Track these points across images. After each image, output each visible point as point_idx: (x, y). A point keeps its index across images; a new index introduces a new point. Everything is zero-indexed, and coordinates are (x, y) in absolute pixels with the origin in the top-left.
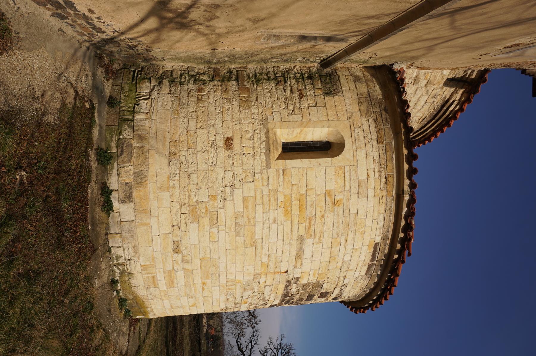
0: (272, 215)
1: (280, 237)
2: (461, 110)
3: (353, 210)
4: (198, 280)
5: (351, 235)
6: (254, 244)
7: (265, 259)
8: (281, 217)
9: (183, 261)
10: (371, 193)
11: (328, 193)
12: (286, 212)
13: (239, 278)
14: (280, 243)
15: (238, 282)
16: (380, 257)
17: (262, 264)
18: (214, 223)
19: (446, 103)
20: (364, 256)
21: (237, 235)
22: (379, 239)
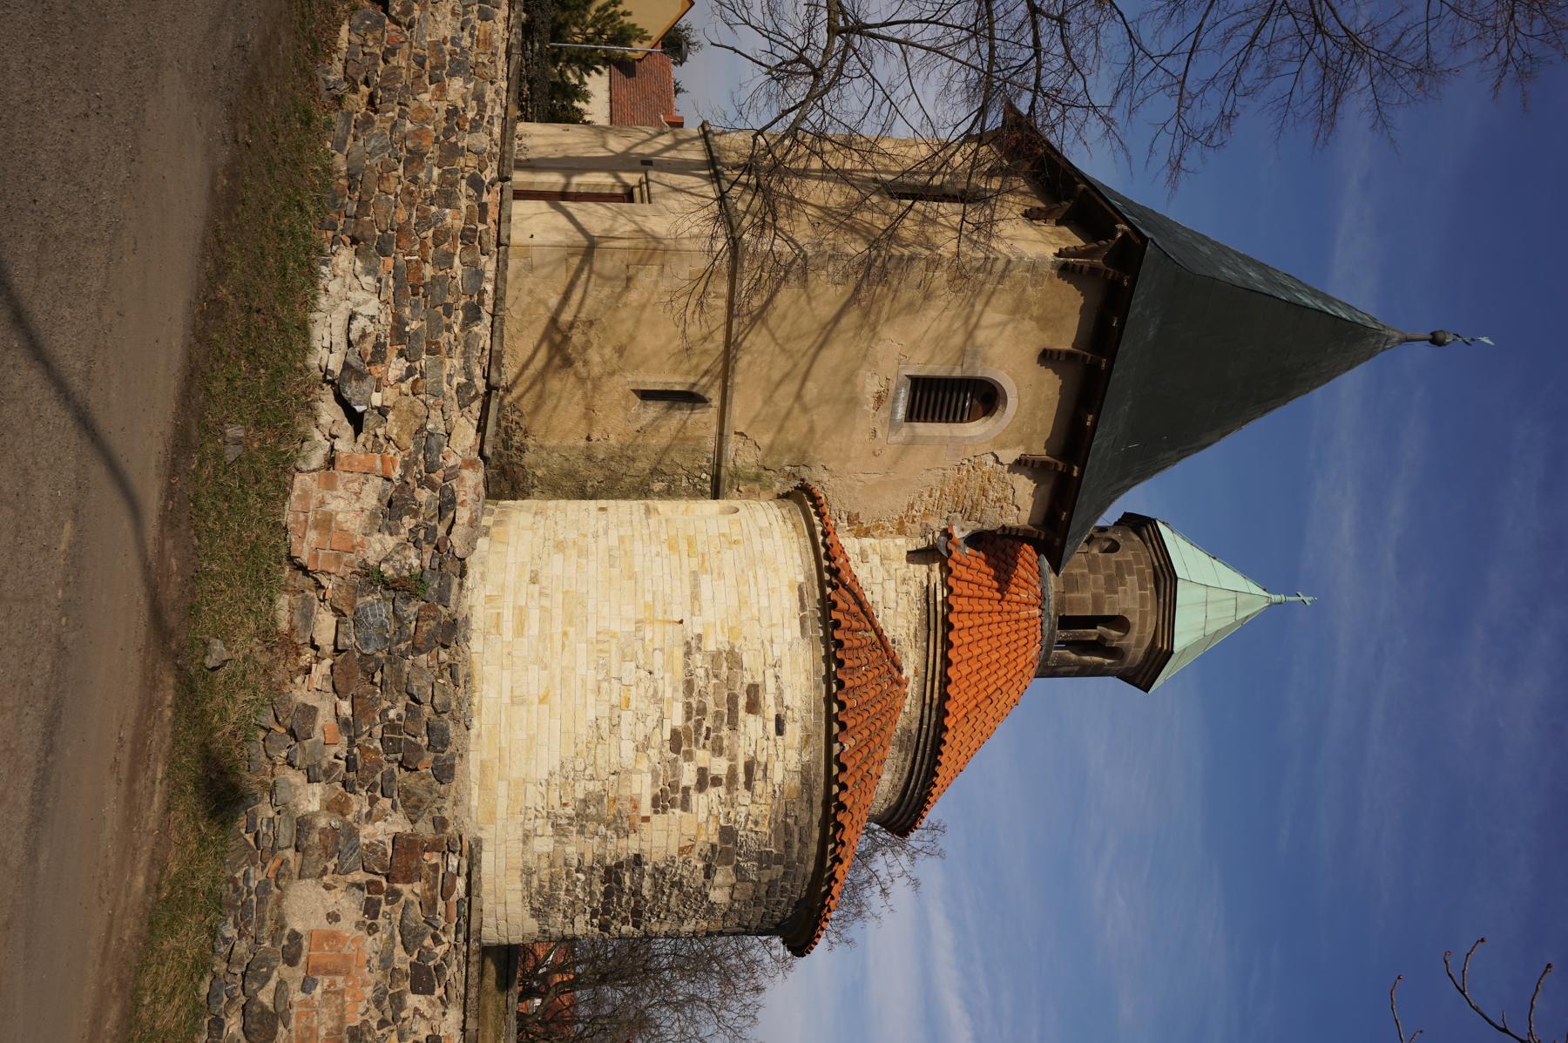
0: (654, 549)
1: (666, 570)
2: (950, 590)
3: (758, 548)
4: (558, 628)
5: (760, 572)
6: (632, 576)
7: (649, 598)
8: (666, 551)
9: (541, 594)
10: (777, 535)
12: (671, 547)
14: (667, 577)
15: (614, 636)
16: (812, 604)
17: (646, 606)
18: (583, 553)
19: (928, 593)
20: (790, 601)
21: (611, 566)
22: (801, 579)
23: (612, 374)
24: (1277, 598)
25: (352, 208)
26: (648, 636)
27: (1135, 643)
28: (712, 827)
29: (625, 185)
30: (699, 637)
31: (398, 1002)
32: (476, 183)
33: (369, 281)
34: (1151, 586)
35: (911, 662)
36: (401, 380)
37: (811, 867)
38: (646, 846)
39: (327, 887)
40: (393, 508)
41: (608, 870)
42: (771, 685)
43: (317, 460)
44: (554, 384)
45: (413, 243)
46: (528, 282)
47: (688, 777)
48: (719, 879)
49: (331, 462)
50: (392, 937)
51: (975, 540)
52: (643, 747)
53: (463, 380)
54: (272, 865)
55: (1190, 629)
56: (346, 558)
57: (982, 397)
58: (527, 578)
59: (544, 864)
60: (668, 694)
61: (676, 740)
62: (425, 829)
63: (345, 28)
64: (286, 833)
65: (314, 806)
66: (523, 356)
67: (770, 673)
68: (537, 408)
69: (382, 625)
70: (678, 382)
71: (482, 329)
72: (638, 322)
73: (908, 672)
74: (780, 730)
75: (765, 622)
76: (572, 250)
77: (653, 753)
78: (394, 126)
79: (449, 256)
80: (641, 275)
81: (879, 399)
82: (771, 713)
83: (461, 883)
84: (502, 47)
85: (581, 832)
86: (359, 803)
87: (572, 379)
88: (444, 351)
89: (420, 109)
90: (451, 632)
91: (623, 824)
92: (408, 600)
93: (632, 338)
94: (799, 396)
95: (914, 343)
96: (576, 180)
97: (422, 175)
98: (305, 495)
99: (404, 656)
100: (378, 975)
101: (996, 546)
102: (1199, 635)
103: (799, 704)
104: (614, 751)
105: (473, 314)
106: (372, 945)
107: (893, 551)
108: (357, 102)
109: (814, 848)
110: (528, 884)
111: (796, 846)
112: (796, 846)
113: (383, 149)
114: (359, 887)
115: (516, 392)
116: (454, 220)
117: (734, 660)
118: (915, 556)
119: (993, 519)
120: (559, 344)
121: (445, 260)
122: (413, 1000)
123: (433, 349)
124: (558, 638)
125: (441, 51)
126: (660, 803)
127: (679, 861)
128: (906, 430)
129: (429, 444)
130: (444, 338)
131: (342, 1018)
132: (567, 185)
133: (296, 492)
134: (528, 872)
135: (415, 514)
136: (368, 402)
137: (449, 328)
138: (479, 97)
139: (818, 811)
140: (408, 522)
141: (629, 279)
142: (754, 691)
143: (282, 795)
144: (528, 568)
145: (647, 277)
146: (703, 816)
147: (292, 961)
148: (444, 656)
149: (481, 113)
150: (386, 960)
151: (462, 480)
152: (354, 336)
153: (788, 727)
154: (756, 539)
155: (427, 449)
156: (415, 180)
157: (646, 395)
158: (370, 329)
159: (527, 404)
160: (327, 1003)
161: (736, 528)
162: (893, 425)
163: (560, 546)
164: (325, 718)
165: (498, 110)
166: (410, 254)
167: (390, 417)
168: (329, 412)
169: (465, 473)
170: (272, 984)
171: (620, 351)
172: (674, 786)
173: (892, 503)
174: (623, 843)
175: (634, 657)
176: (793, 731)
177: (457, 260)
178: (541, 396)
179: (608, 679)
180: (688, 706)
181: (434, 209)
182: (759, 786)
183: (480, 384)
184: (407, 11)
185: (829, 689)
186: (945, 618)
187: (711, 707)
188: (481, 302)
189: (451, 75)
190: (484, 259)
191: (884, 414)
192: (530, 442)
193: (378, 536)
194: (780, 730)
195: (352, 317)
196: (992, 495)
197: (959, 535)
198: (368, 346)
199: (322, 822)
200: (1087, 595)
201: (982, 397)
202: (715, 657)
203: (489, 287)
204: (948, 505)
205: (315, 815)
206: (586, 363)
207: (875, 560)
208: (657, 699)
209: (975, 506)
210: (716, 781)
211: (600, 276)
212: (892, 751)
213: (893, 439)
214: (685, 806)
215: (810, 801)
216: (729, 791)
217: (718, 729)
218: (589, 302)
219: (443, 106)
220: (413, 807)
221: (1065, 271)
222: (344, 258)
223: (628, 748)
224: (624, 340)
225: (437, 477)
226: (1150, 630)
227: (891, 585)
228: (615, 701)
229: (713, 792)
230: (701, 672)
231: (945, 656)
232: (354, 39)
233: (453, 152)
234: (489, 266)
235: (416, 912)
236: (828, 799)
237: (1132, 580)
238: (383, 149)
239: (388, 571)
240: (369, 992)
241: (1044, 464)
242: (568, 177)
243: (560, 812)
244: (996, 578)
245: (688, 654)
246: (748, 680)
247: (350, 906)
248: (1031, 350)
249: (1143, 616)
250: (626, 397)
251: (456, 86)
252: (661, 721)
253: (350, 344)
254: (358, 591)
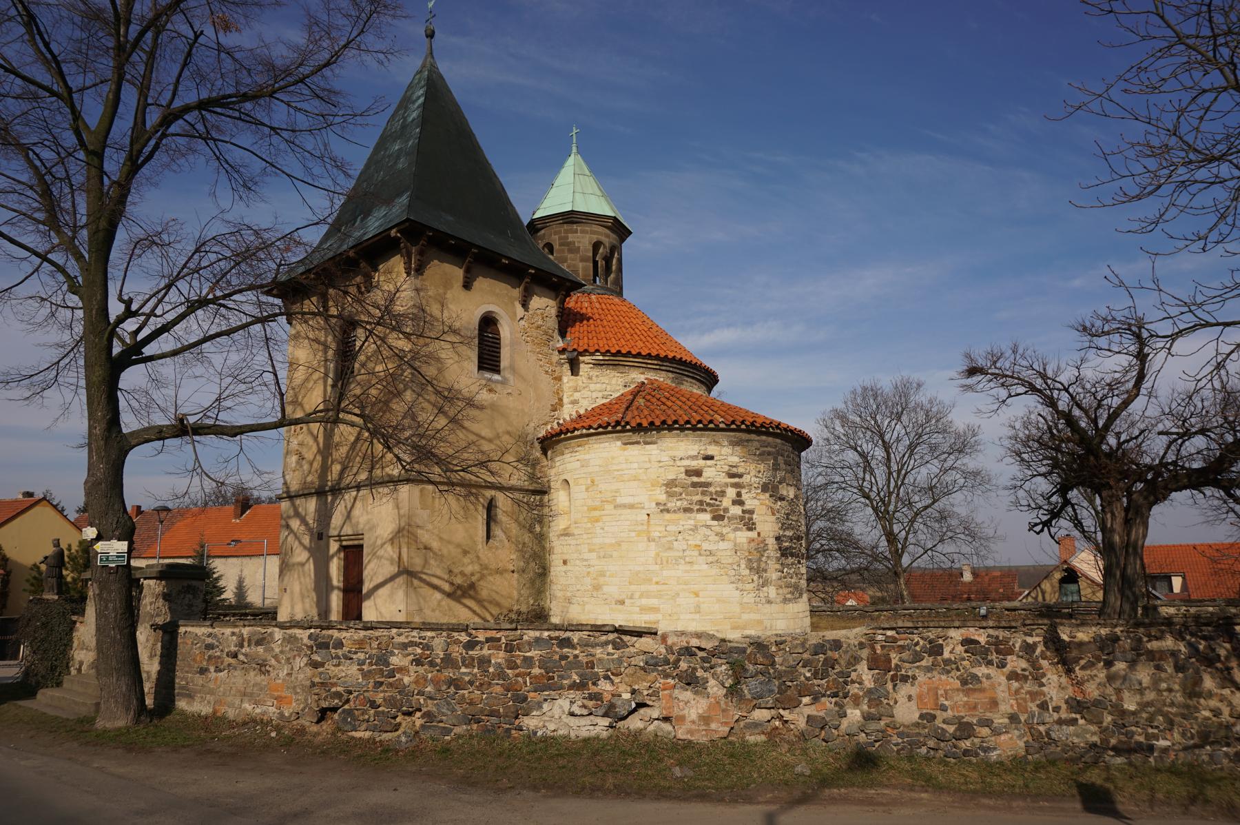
0: (598, 531)
2: (597, 351)
3: (597, 469)
4: (654, 588)
5: (615, 467)
6: (619, 544)
7: (633, 534)
8: (600, 524)
10: (587, 457)
11: (587, 489)
12: (597, 521)
13: (653, 554)
16: (636, 437)
17: (638, 535)
18: (602, 574)
19: (598, 364)
20: (634, 450)
23: (478, 557)
24: (574, 150)
25: (494, 720)
26: (658, 534)
27: (608, 238)
28: (762, 497)
29: (339, 551)
30: (658, 504)
31: (947, 662)
32: (471, 645)
33: (546, 706)
34: (575, 226)
35: (638, 376)
36: (612, 682)
37: (779, 441)
38: (772, 534)
39: (896, 702)
40: (691, 681)
41: (782, 555)
42: (686, 463)
43: (667, 727)
44: (484, 594)
45: (517, 682)
46: (428, 612)
47: (736, 510)
48: (785, 493)
49: (666, 719)
50: (917, 667)
51: (563, 334)
52: (722, 537)
53: (610, 646)
54: (890, 731)
55: (601, 207)
56: (724, 706)
57: (488, 323)
58: (620, 607)
59: (781, 591)
60: (692, 522)
61: (718, 518)
62: (865, 653)
63: (354, 734)
64: (873, 726)
65: (858, 712)
66: (468, 614)
67: (679, 463)
68: (498, 604)
69: (761, 683)
70: (481, 516)
71: (575, 637)
72: (449, 542)
73: (641, 378)
74: (712, 458)
75: (648, 465)
76: (409, 585)
77: (725, 531)
78: (431, 698)
79: (526, 658)
80: (424, 540)
81: (490, 390)
82: (702, 462)
83: (889, 633)
84: (362, 633)
85: (765, 571)
86: (854, 689)
87: (481, 583)
88: (591, 658)
89: (416, 682)
90: (759, 645)
91: (761, 548)
92: (746, 670)
93: (458, 546)
94: (490, 441)
95: (461, 370)
96: (335, 583)
97: (467, 679)
98: (690, 732)
99: (776, 670)
100: (935, 673)
101: (567, 320)
102: (603, 199)
103: (696, 447)
104: (724, 553)
105: (566, 643)
106: (922, 678)
107: (571, 384)
109: (770, 439)
110: (790, 600)
111: (769, 449)
112: (769, 449)
113: (448, 704)
114: (895, 686)
115: (489, 617)
116: (499, 657)
117: (670, 484)
118: (574, 370)
119: (553, 323)
120: (463, 592)
121: (528, 661)
122: (946, 655)
123: (591, 665)
124: (659, 587)
125: (369, 671)
126: (751, 527)
127: (778, 515)
128: (506, 373)
130: (583, 658)
131: (958, 690)
132: (338, 588)
133: (689, 737)
134: (785, 600)
135: (695, 669)
136: (629, 701)
137: (576, 656)
138: (404, 646)
139: (753, 436)
140: (700, 673)
141: (426, 548)
142: (689, 473)
143: (854, 730)
144: (614, 606)
145: (424, 537)
146: (756, 502)
147: (934, 717)
148: (774, 649)
149: (417, 644)
150: (928, 669)
151: (674, 644)
152: (585, 712)
153: (710, 453)
154: (590, 469)
155: (656, 665)
156: (471, 683)
157: (488, 537)
158: (580, 703)
159: (495, 611)
160: (952, 698)
161: (581, 481)
162: (504, 382)
163: (597, 588)
164: (812, 711)
165: (415, 633)
166: (525, 683)
167: (636, 687)
168: (634, 723)
169: (670, 642)
170: (945, 726)
171: (465, 553)
172: (742, 519)
173: (545, 382)
174: (770, 547)
175: (670, 542)
176: (712, 450)
177: (528, 654)
178: (491, 602)
179: (684, 558)
180: (698, 510)
181: (491, 670)
182: (741, 470)
183: (611, 636)
184: (338, 695)
185: (700, 429)
186: (614, 355)
187: (699, 497)
188: (557, 638)
189: (388, 664)
190: (525, 638)
191: (499, 388)
192: (515, 608)
193: (709, 689)
194: (712, 458)
195: (572, 714)
196: (540, 323)
197: (561, 345)
198: (590, 704)
199: (865, 707)
200: (581, 265)
202: (670, 495)
203: (546, 634)
204: (545, 349)
205: (862, 713)
206: (472, 574)
207: (577, 395)
208: (695, 529)
209: (546, 333)
210: (739, 494)
211: (424, 567)
212: (683, 387)
213: (512, 382)
214: (751, 512)
215: (748, 441)
216: (743, 487)
217: (711, 494)
218: (439, 572)
219: (413, 668)
220: (856, 660)
221: (420, 270)
223: (723, 545)
224: (459, 550)
225: (672, 658)
226: (601, 229)
227: (592, 387)
228: (696, 553)
229: (744, 497)
230: (679, 503)
231: (634, 356)
232: (363, 727)
233: (448, 661)
235: (905, 655)
236: (748, 431)
237: (571, 238)
238: (448, 704)
239: (729, 682)
240: (944, 677)
241: (526, 290)
242: (333, 588)
243: (755, 584)
244: (581, 321)
245: (668, 511)
246: (683, 476)
247: (905, 690)
248: (463, 294)
249: (593, 232)
250: (490, 548)
251: (396, 660)
252: (708, 527)
253: (591, 714)
254: (741, 697)
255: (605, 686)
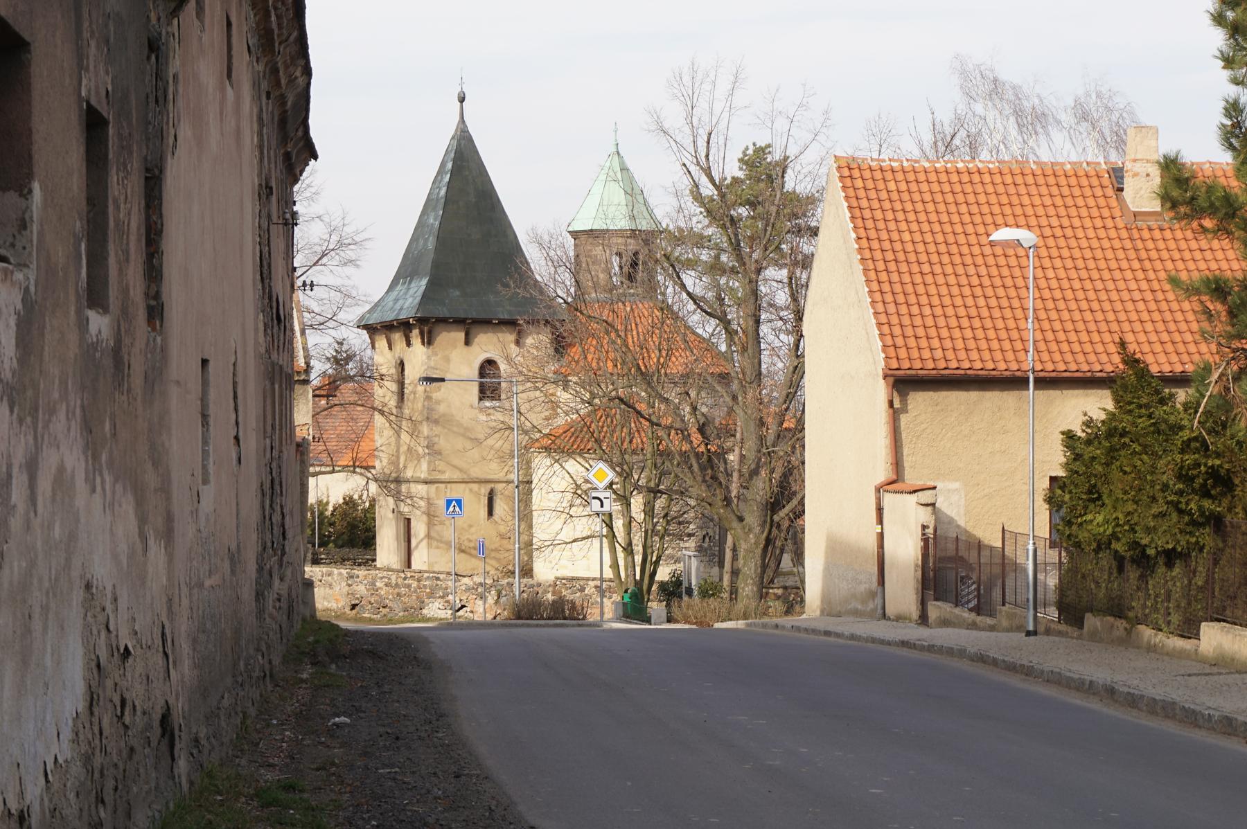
32: (405, 579)
40: (482, 597)
105: (438, 579)
108: (384, 611)
116: (415, 584)
129: (468, 589)
168: (461, 613)
201: (488, 366)
222: (425, 611)
233: (397, 584)
234: (426, 575)
248: (465, 349)
255: (451, 597)
